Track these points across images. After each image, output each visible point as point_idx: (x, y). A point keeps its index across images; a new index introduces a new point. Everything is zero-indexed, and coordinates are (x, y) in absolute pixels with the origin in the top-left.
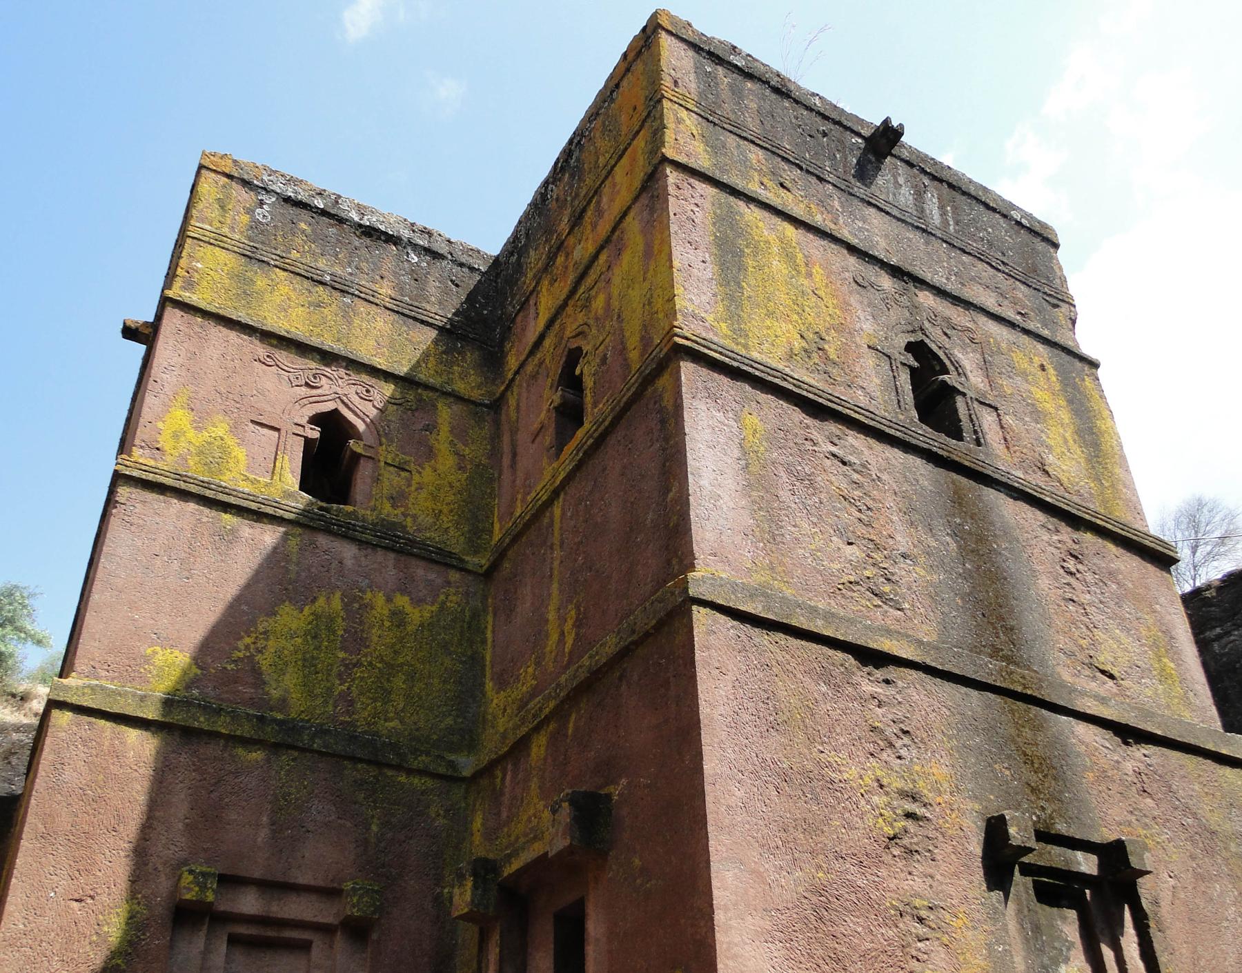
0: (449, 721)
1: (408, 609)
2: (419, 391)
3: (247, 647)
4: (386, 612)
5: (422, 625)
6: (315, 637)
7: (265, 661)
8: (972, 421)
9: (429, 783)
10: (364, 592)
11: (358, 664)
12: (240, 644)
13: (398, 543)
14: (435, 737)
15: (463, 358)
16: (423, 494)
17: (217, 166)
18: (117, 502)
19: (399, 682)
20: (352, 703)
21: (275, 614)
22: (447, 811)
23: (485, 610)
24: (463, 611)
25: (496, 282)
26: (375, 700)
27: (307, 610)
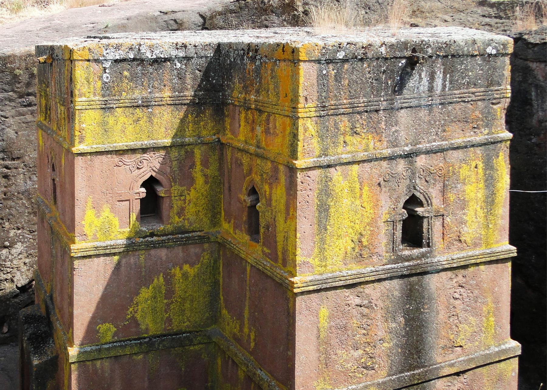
0: (207, 315)
1: (189, 270)
2: (186, 147)
3: (131, 312)
4: (180, 275)
5: (195, 276)
6: (155, 298)
7: (138, 316)
8: (428, 232)
9: (201, 346)
10: (170, 270)
11: (172, 302)
12: (129, 312)
13: (183, 241)
14: (202, 324)
15: (205, 115)
16: (191, 205)
17: (82, 57)
18: (75, 268)
19: (187, 305)
20: (171, 320)
21: (139, 293)
22: (208, 355)
23: (219, 258)
24: (210, 262)
25: (219, 60)
26: (179, 316)
27: (150, 287)
